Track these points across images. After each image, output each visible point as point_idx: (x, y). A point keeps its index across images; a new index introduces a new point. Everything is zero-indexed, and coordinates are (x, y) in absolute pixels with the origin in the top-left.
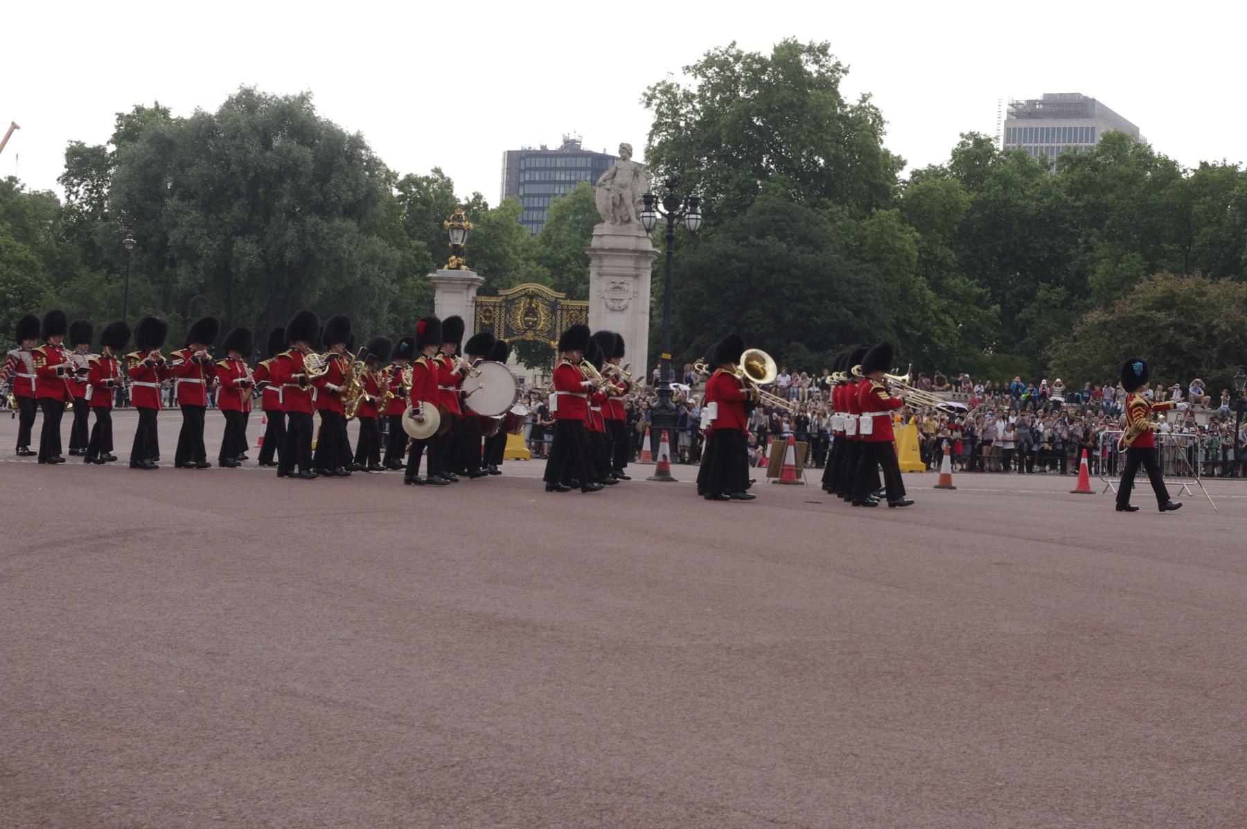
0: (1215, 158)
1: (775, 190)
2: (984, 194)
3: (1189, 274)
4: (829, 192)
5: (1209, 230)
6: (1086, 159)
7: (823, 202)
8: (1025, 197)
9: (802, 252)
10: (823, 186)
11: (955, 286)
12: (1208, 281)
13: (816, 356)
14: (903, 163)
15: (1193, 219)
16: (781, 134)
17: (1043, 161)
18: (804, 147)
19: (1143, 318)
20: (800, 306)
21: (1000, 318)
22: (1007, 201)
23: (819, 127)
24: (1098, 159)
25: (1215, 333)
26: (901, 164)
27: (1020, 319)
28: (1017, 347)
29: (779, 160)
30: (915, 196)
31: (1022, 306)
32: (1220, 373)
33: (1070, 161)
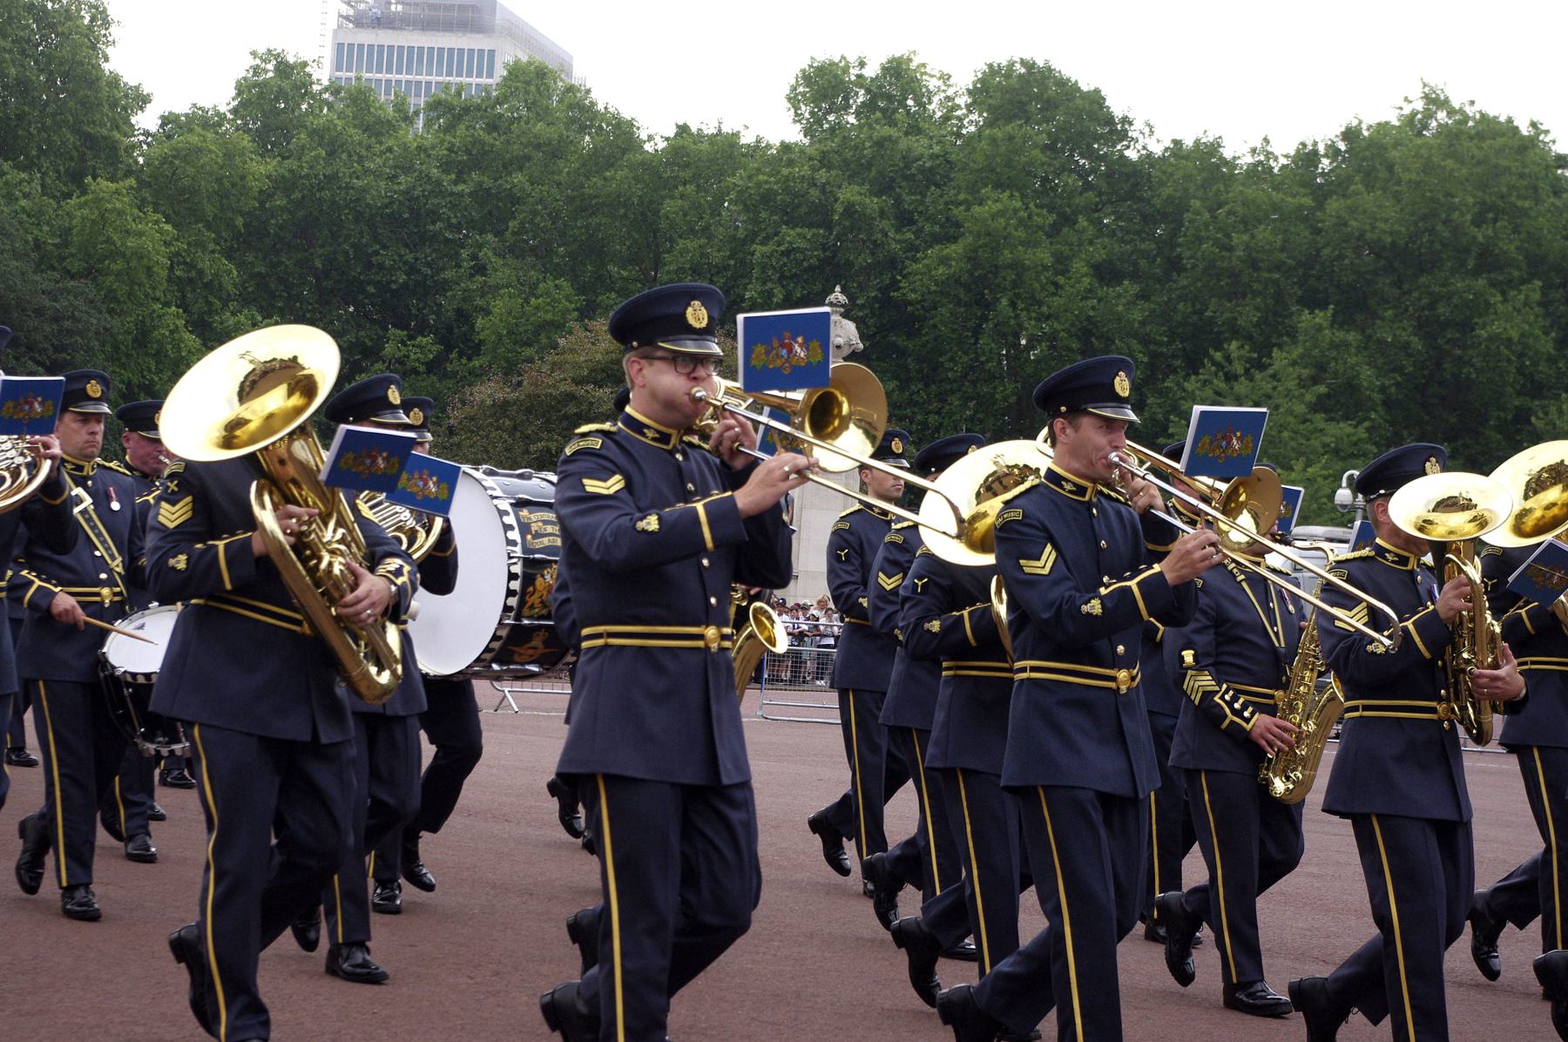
2: (291, 164)
5: (691, 244)
6: (478, 108)
8: (367, 171)
15: (663, 225)
17: (400, 106)
19: (571, 397)
22: (332, 178)
24: (499, 109)
26: (142, 100)
30: (165, 160)
33: (449, 110)
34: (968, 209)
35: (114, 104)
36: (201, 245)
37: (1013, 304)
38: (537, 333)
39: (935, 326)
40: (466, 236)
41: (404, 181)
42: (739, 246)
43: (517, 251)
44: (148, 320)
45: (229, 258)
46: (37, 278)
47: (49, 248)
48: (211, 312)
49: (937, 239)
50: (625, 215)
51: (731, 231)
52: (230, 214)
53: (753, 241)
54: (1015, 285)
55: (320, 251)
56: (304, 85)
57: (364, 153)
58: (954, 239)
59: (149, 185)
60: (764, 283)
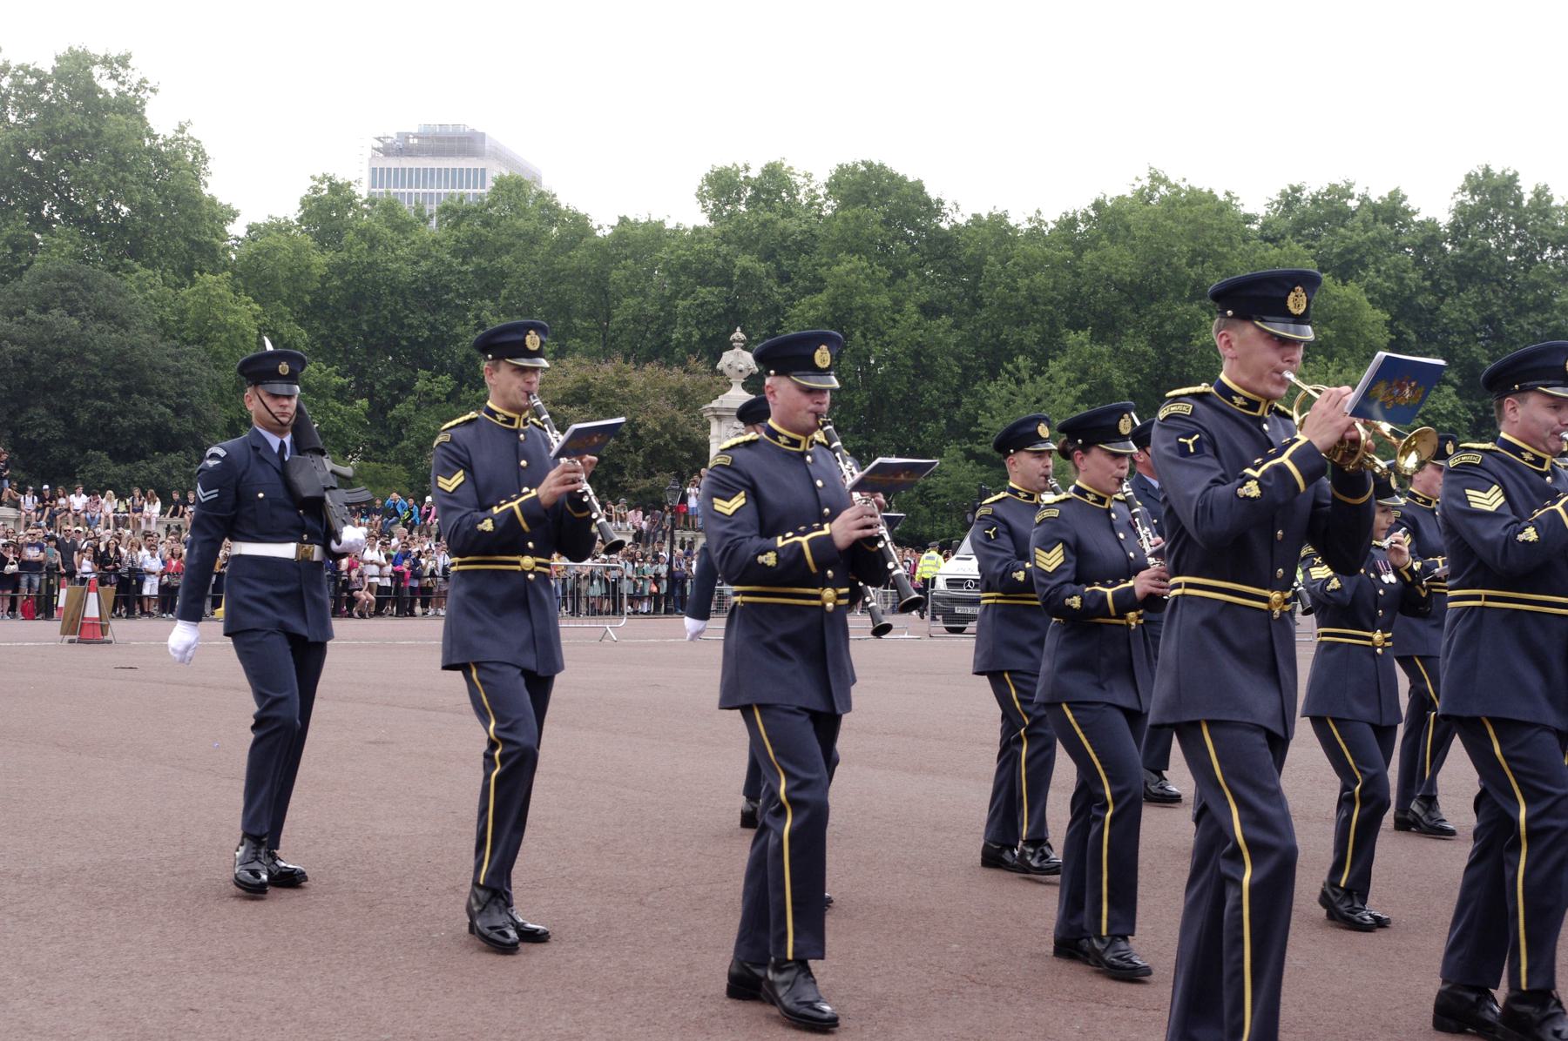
0: (639, 213)
1: (61, 247)
3: (608, 358)
4: (134, 253)
5: (631, 301)
6: (475, 210)
9: (100, 331)
10: (128, 244)
12: (631, 366)
13: (122, 469)
14: (236, 214)
15: (611, 288)
16: (67, 173)
18: (98, 190)
20: (99, 403)
21: (368, 415)
23: (123, 166)
25: (641, 432)
27: (394, 418)
28: (392, 454)
29: (69, 209)
30: (251, 257)
31: (396, 400)
32: (648, 483)
33: (454, 214)
35: (213, 218)
36: (281, 316)
37: (864, 336)
42: (667, 302)
54: (865, 321)
56: (350, 200)
58: (820, 291)
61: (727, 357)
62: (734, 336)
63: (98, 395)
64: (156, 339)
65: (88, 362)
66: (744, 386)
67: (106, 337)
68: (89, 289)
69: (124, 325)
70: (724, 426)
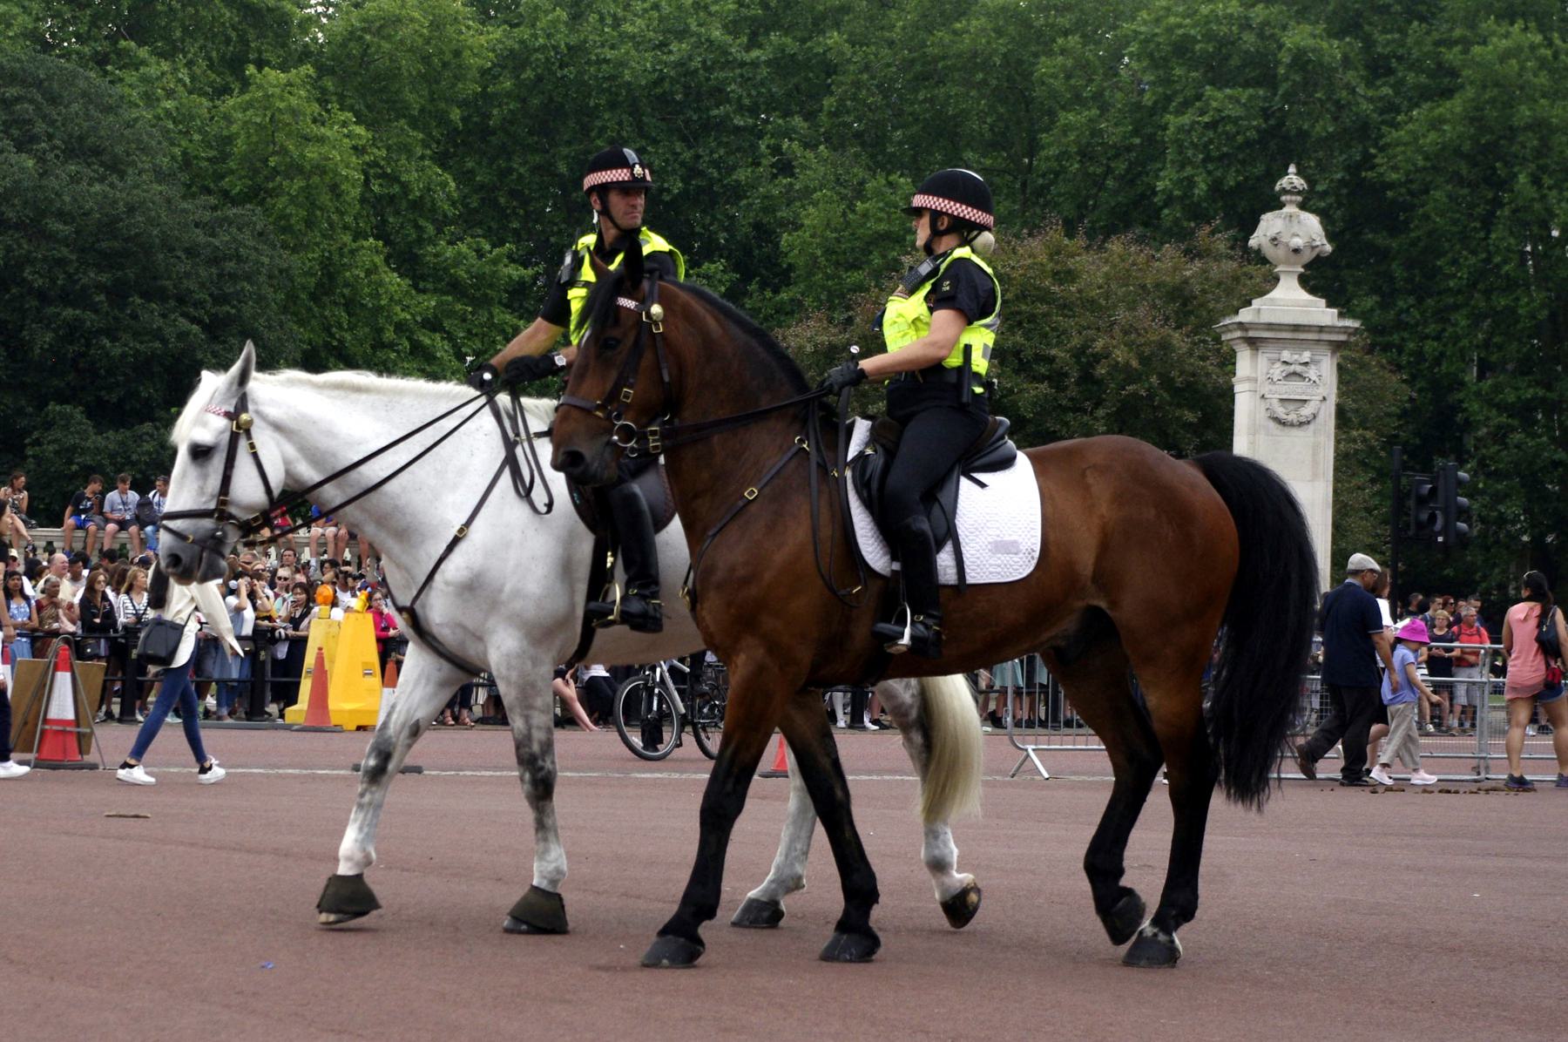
2: (524, 32)
4: (138, 31)
7: (121, 53)
9: (75, 179)
11: (458, 260)
12: (1081, 241)
13: (111, 439)
15: (1038, 92)
20: (69, 313)
25: (1101, 371)
30: (352, 35)
34: (1466, 51)
36: (406, 149)
37: (1536, 181)
38: (866, 252)
39: (1426, 217)
40: (766, 121)
41: (679, 49)
42: (1146, 119)
43: (836, 141)
44: (336, 257)
45: (443, 166)
46: (185, 205)
47: (204, 164)
48: (420, 241)
49: (1425, 95)
50: (985, 82)
51: (1134, 98)
52: (443, 105)
53: (1165, 109)
54: (1539, 154)
55: (565, 151)
57: (620, 13)
58: (1447, 93)
59: (332, 72)
60: (1182, 167)
61: (1270, 225)
62: (1284, 182)
63: (66, 298)
64: (174, 192)
65: (50, 237)
66: (1304, 281)
67: (96, 193)
68: (54, 100)
69: (116, 167)
70: (1262, 359)
